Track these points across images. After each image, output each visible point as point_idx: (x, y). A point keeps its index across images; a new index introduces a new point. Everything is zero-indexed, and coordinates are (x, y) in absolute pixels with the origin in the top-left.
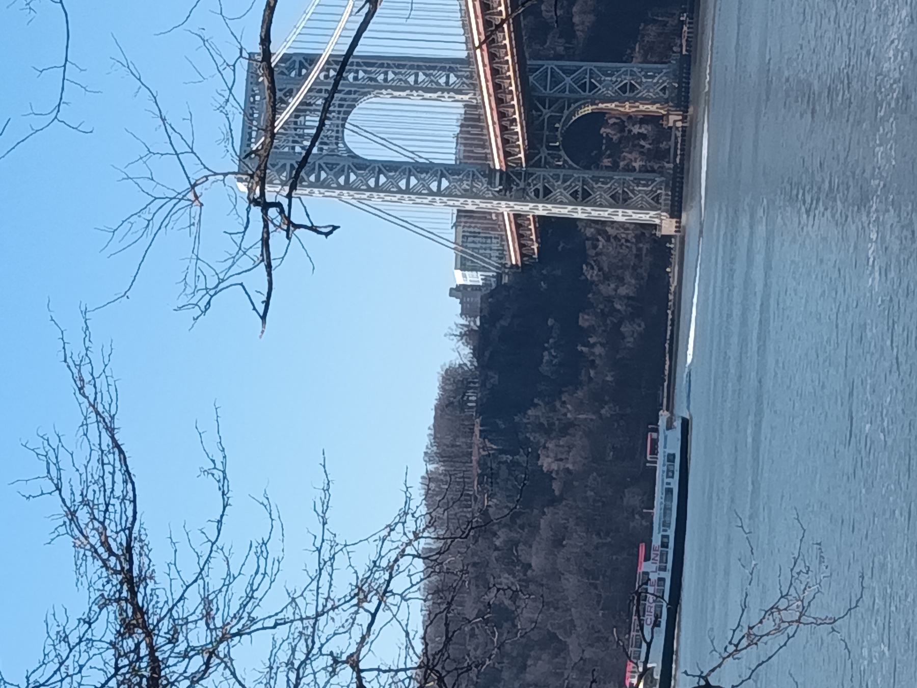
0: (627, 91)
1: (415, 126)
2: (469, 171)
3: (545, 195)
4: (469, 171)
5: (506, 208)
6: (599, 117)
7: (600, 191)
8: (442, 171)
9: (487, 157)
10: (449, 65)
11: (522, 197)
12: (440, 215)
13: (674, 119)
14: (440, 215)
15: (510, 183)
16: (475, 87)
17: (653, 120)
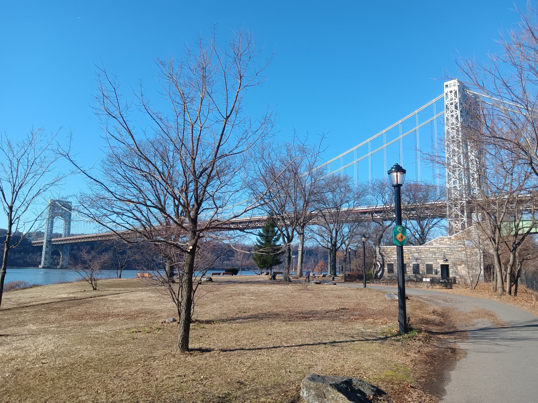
0: (63, 260)
1: (59, 226)
2: (51, 235)
3: (47, 247)
4: (51, 235)
5: (45, 241)
6: (59, 255)
7: (47, 256)
8: (51, 231)
9: (54, 238)
10: (69, 232)
11: (47, 243)
12: (44, 229)
13: (59, 267)
14: (44, 229)
15: (49, 242)
16: (65, 236)
17: (58, 264)
